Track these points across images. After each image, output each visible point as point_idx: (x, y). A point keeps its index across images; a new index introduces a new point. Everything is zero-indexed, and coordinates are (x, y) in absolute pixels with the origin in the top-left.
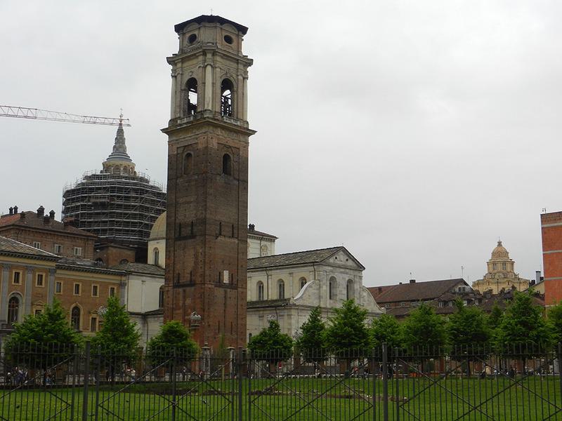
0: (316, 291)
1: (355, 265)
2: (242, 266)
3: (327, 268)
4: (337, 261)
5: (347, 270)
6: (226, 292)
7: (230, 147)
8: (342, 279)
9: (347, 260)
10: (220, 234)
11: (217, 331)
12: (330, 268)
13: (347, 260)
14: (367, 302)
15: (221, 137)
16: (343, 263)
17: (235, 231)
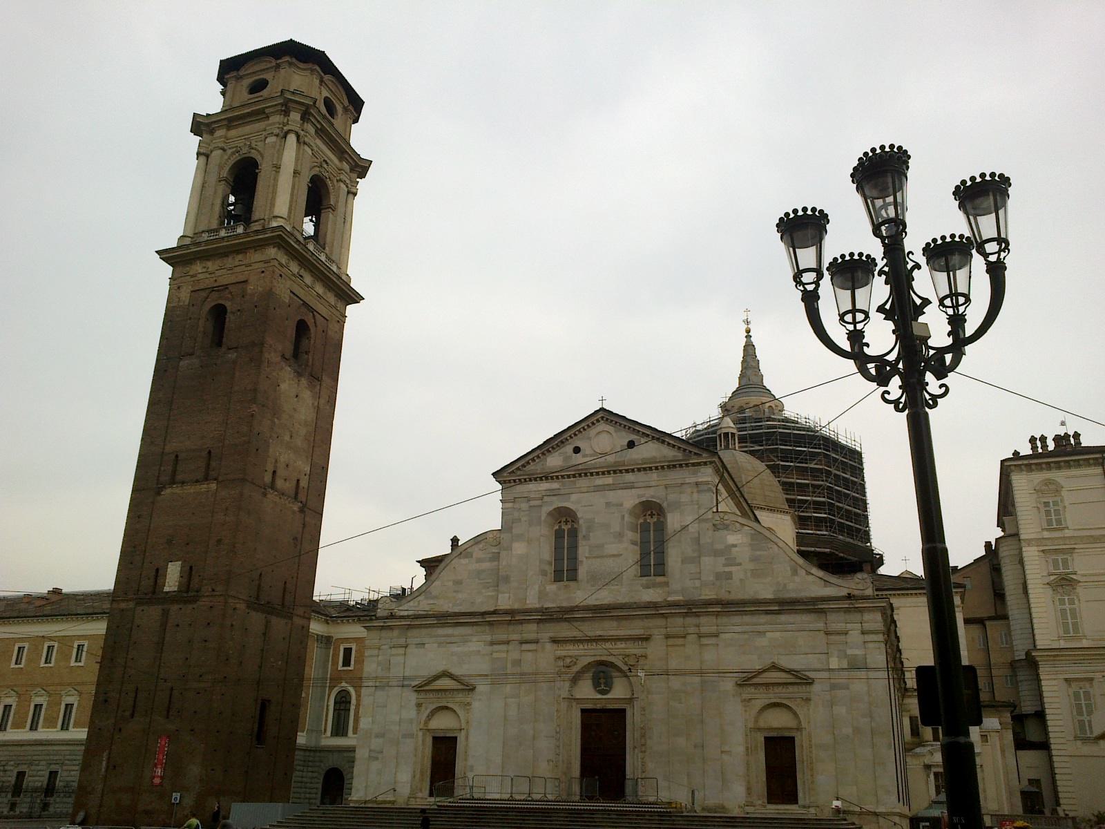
0: (486, 565)
1: (669, 453)
2: (219, 541)
3: (532, 486)
4: (578, 459)
5: (630, 477)
6: (165, 613)
7: (226, 287)
9: (631, 445)
10: (173, 482)
11: (127, 714)
12: (545, 486)
13: (631, 445)
14: (751, 566)
15: (201, 276)
16: (611, 459)
17: (213, 464)
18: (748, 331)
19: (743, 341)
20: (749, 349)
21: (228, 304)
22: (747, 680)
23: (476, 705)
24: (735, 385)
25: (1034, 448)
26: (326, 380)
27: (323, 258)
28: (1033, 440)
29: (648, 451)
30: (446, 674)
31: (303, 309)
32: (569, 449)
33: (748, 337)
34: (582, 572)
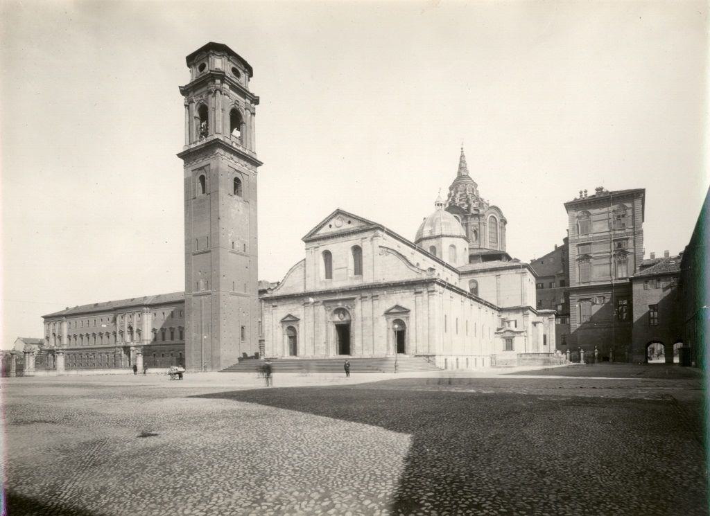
8: (341, 250)
18: (462, 149)
19: (460, 154)
20: (462, 156)
21: (204, 174)
22: (388, 313)
23: (301, 325)
24: (455, 176)
25: (581, 196)
26: (252, 202)
27: (241, 148)
28: (581, 192)
29: (354, 226)
30: (289, 316)
31: (236, 173)
32: (328, 226)
33: (462, 152)
34: (334, 275)
